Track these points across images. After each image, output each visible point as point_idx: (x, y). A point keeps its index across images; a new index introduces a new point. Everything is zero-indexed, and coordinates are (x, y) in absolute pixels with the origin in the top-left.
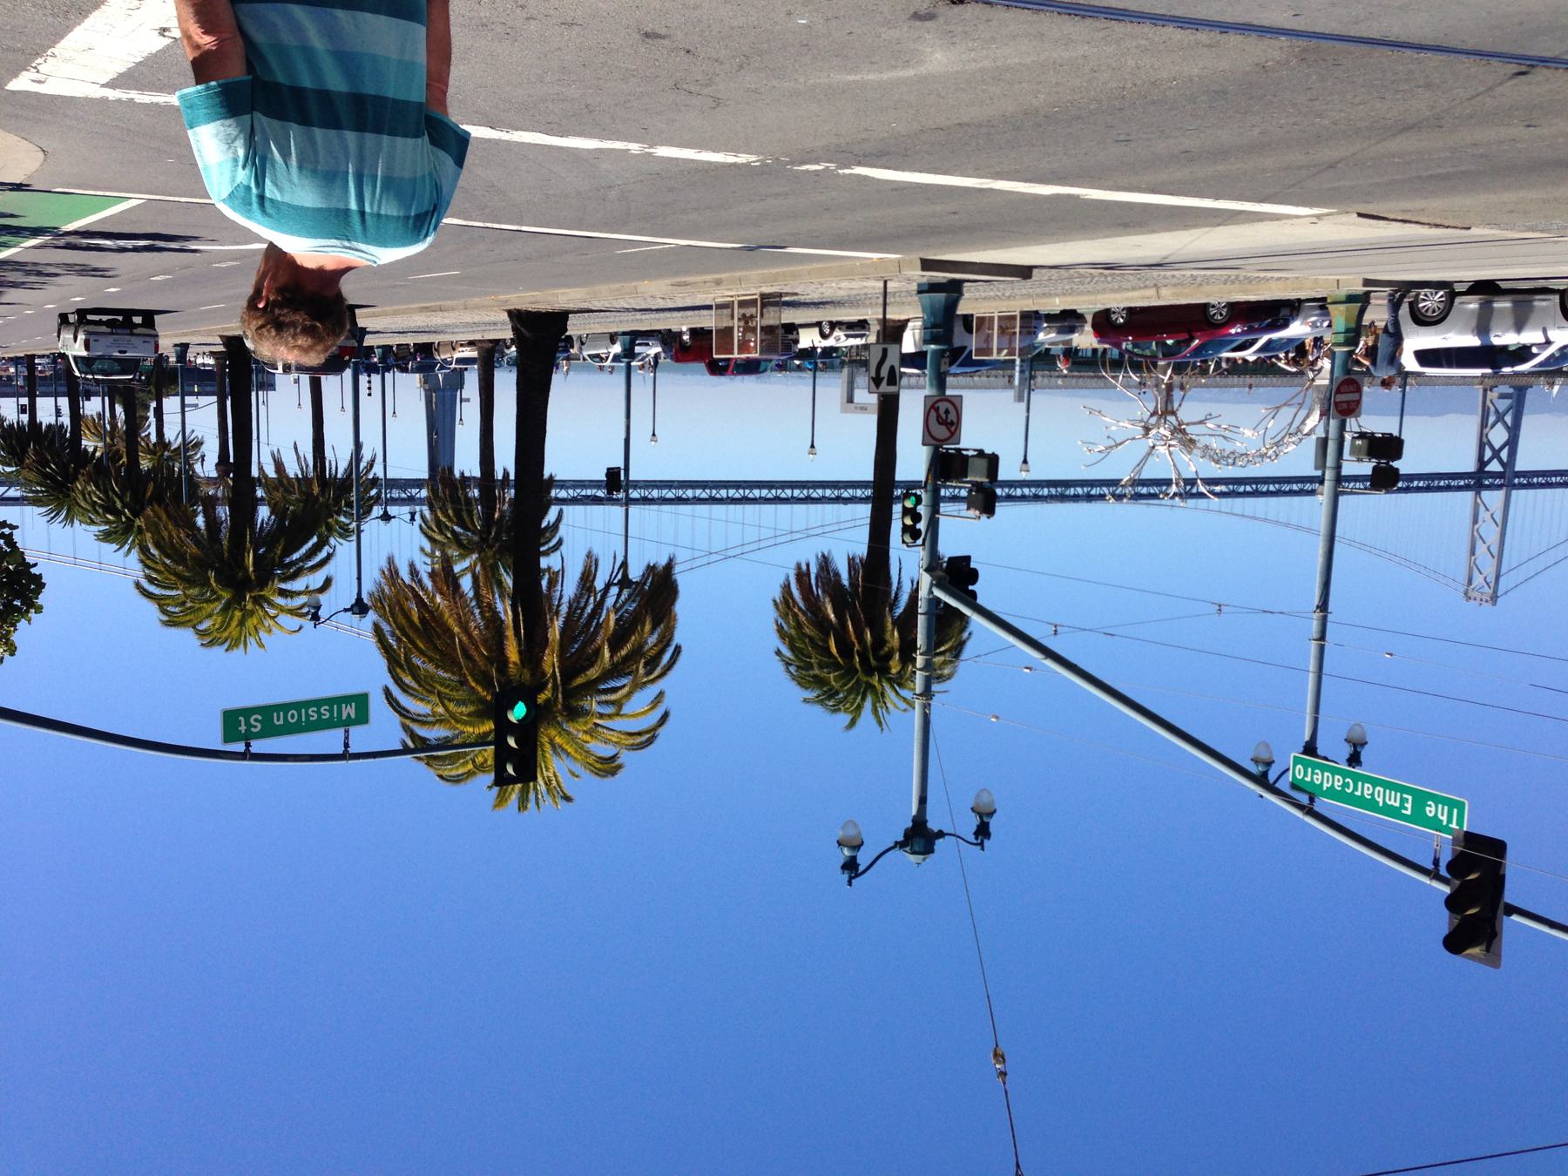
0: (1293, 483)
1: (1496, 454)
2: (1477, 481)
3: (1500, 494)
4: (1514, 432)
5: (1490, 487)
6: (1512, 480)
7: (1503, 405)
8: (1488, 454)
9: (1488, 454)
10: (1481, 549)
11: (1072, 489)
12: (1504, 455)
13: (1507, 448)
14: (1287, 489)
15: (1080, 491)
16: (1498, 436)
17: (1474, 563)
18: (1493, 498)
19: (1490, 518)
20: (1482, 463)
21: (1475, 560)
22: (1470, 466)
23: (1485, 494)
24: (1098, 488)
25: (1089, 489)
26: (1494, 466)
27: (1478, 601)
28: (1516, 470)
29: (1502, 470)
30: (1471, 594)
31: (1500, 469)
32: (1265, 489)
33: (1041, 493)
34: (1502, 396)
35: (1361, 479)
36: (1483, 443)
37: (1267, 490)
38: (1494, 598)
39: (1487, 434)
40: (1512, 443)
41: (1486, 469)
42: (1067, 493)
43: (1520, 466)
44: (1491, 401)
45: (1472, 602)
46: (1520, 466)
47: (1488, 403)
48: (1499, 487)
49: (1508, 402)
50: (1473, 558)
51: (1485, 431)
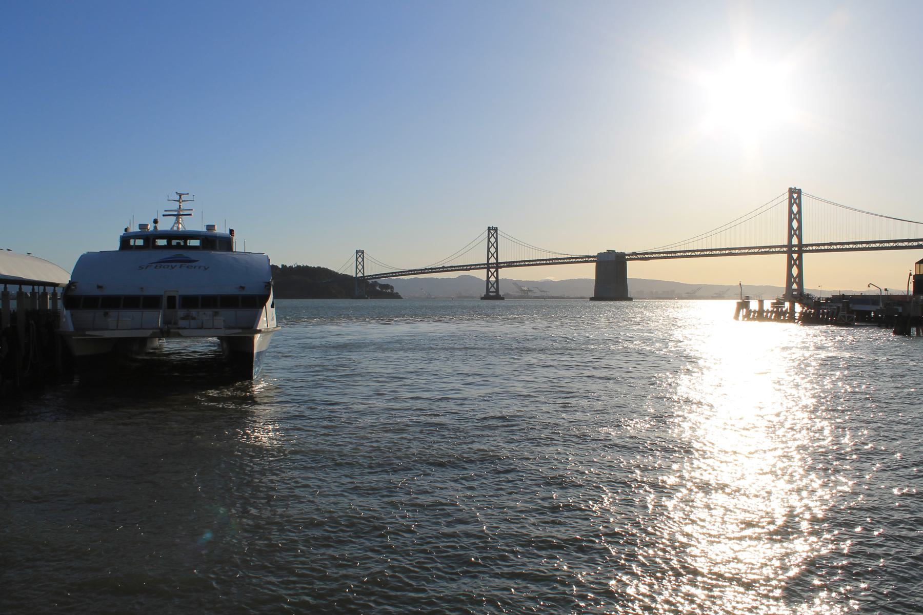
1: (493, 274)
2: (498, 266)
3: (490, 262)
5: (493, 264)
6: (488, 266)
9: (495, 274)
12: (490, 274)
16: (493, 279)
18: (493, 260)
23: (495, 262)
26: (493, 270)
38: (489, 229)
40: (488, 278)
43: (485, 270)
46: (485, 270)
48: (491, 264)
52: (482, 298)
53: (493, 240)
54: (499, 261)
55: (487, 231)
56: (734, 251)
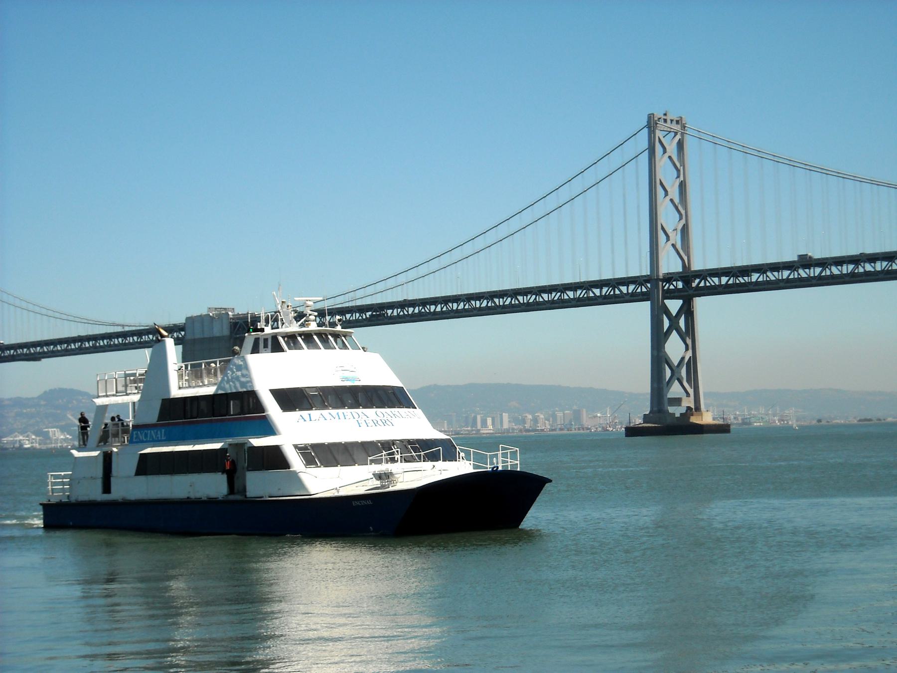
0: (574, 299)
1: (674, 325)
4: (659, 359)
7: (675, 390)
8: (682, 323)
9: (682, 323)
10: (674, 193)
11: (845, 272)
13: (665, 331)
14: (579, 292)
15: (835, 271)
17: (678, 170)
19: (670, 235)
20: (688, 311)
21: (678, 177)
22: (701, 304)
24: (812, 275)
25: (823, 274)
27: (668, 118)
28: (649, 302)
29: (666, 301)
30: (677, 128)
31: (668, 302)
32: (605, 290)
33: (885, 264)
34: (677, 401)
35: (782, 284)
36: (688, 335)
37: (601, 289)
39: (687, 349)
41: (679, 302)
42: (851, 267)
44: (688, 394)
45: (675, 119)
47: (691, 391)
49: (671, 395)
50: (682, 178)
51: (689, 354)
52: (632, 432)
53: (666, 172)
54: (697, 265)
55: (646, 130)
56: (879, 266)
